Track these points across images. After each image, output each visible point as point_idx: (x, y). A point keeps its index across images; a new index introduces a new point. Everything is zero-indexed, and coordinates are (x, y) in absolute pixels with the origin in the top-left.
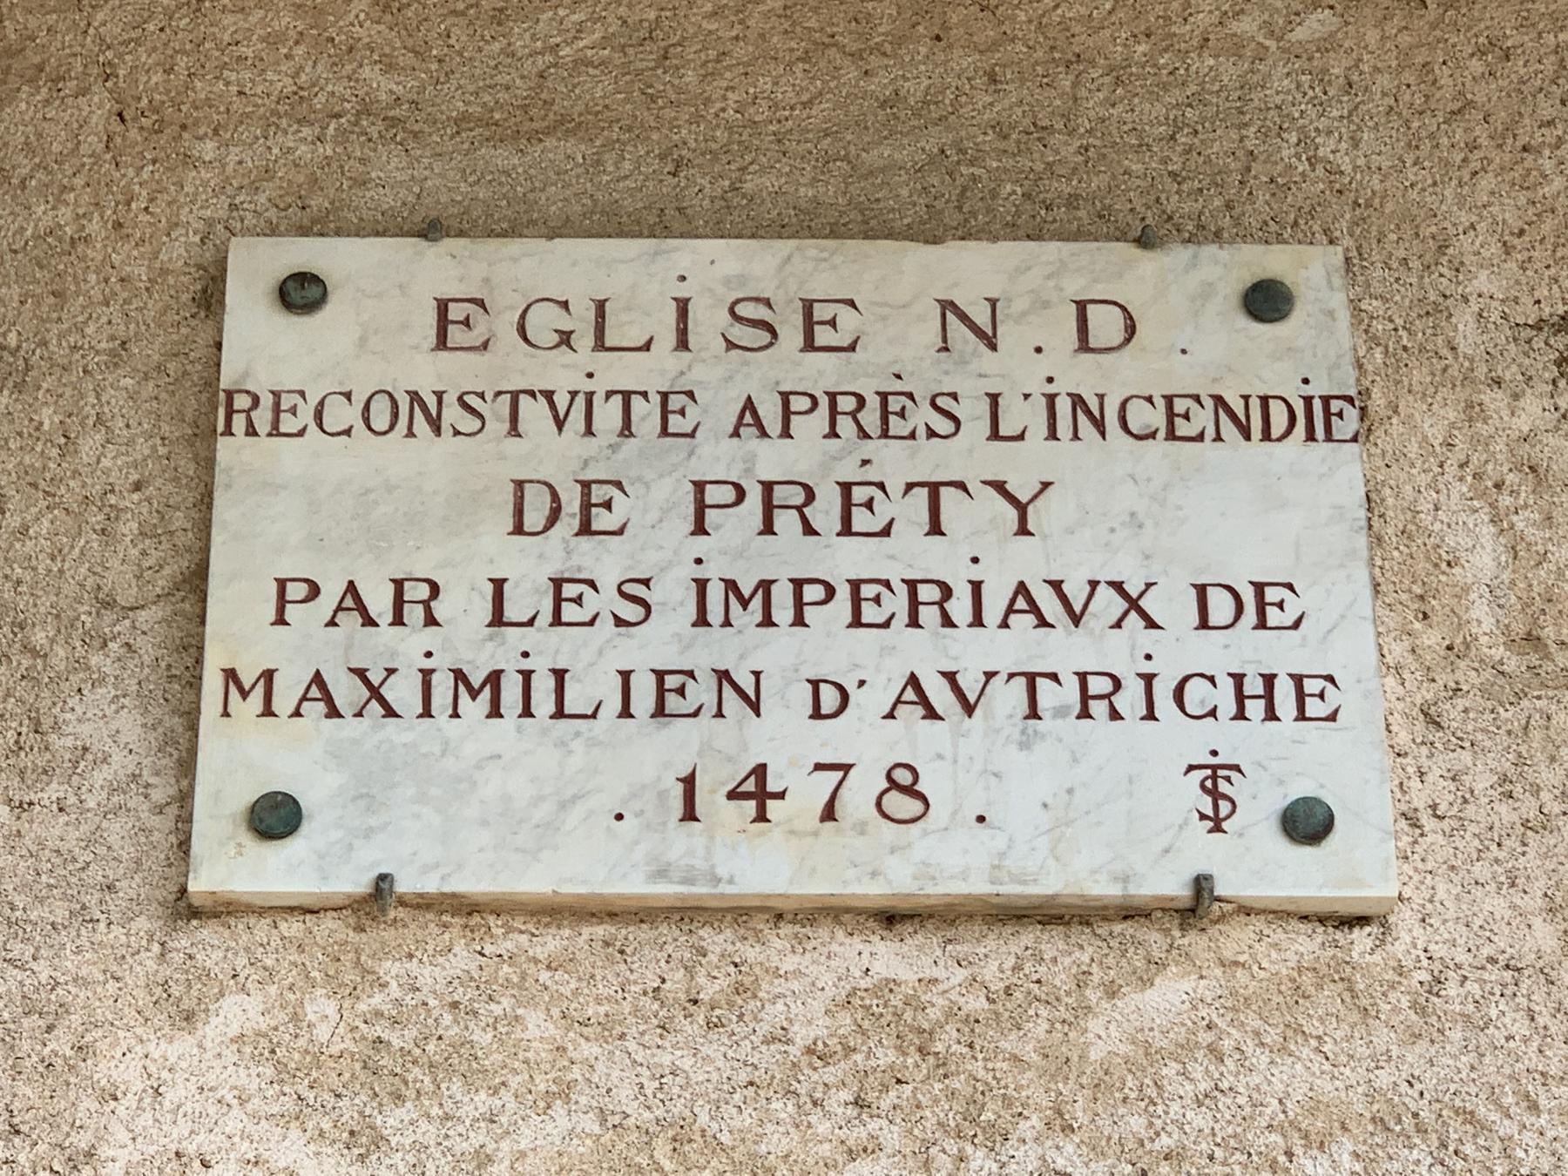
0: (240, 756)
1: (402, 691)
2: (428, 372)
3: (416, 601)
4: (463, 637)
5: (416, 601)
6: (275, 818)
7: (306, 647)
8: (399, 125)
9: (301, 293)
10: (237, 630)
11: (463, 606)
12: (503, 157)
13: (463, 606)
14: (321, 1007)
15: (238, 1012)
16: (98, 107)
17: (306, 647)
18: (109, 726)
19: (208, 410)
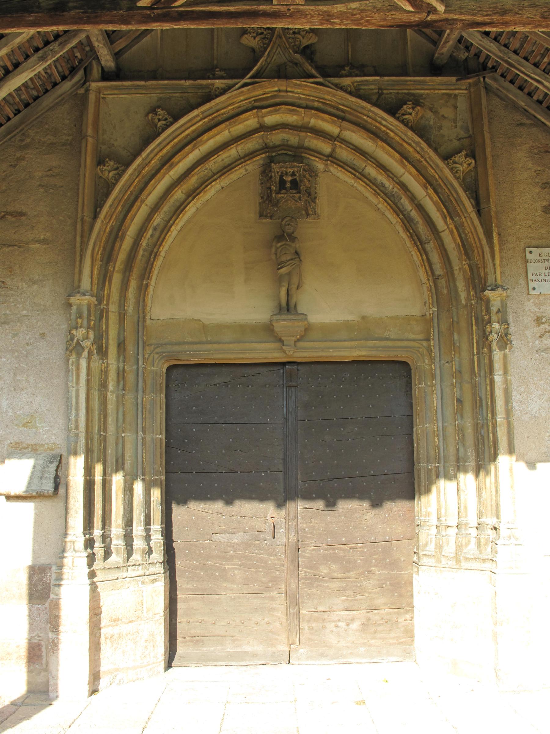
0: (531, 285)
1: (540, 280)
2: (539, 258)
3: (540, 274)
4: (543, 277)
5: (540, 274)
6: (534, 289)
7: (534, 277)
8: (533, 238)
9: (531, 252)
10: (530, 276)
11: (543, 275)
12: (540, 241)
13: (543, 275)
14: (536, 300)
15: (532, 301)
16: (515, 237)
17: (534, 277)
18: (522, 282)
19: (526, 261)
